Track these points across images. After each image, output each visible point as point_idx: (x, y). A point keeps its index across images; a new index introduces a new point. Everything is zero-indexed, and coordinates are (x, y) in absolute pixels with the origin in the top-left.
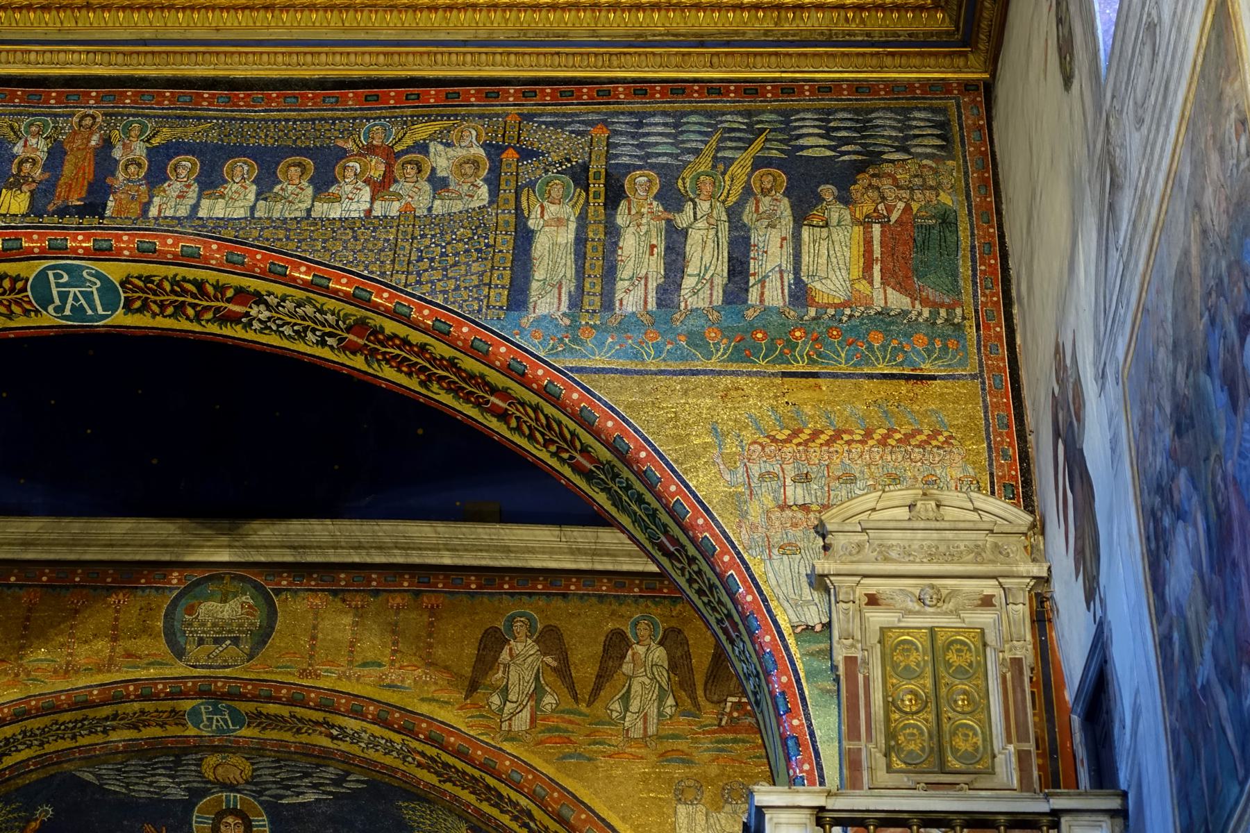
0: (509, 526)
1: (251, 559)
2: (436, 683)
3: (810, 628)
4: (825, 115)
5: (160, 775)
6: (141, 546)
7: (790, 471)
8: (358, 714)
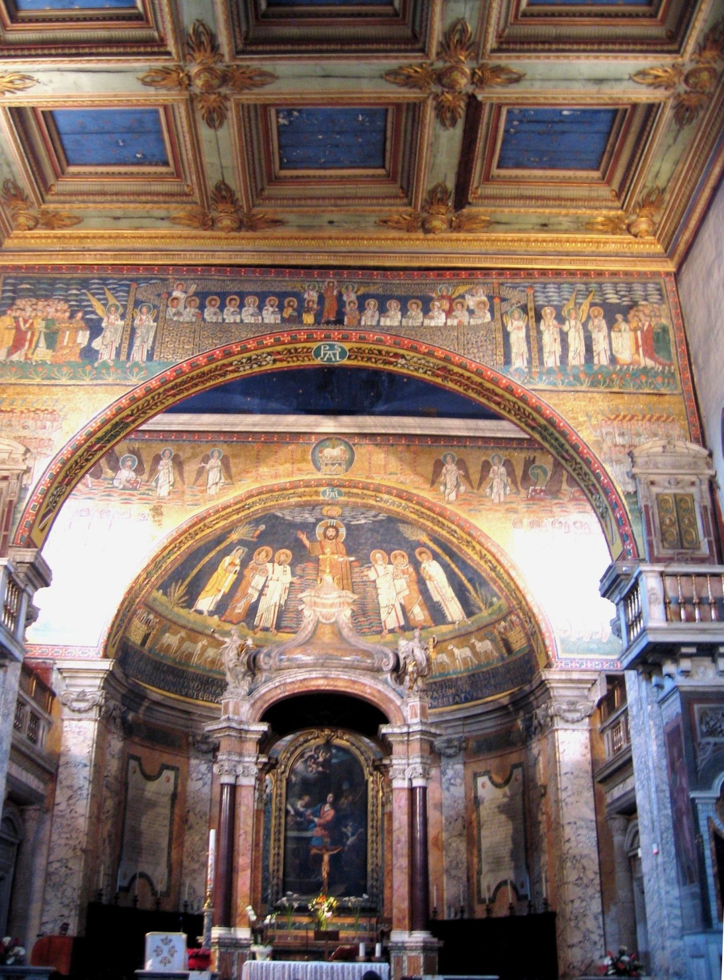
3: (629, 493)
4: (615, 284)
7: (617, 432)
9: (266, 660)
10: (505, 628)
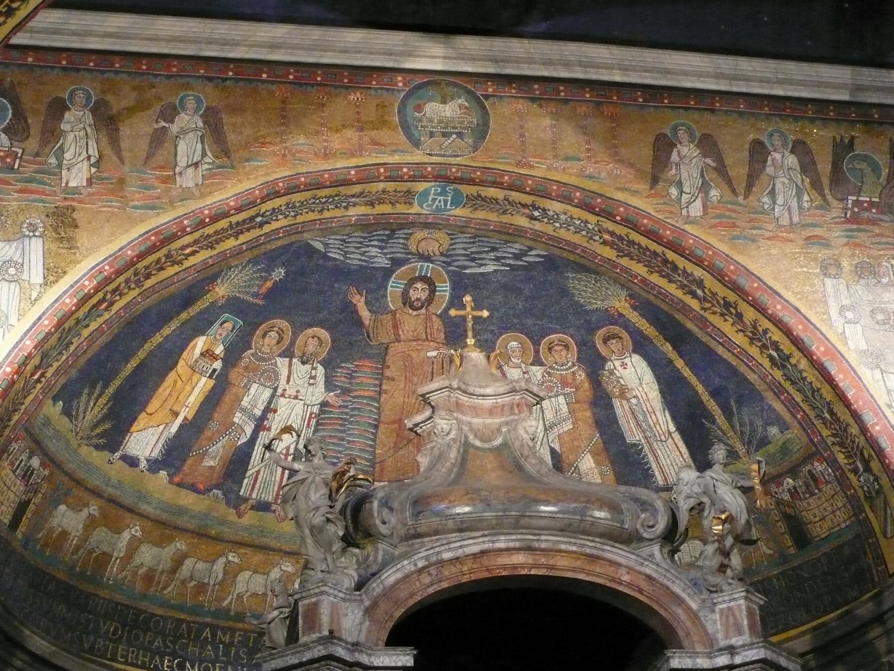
0: (669, 52)
1: (460, 69)
2: (625, 176)
5: (373, 246)
6: (372, 53)
8: (566, 199)
9: (386, 511)
10: (794, 492)
